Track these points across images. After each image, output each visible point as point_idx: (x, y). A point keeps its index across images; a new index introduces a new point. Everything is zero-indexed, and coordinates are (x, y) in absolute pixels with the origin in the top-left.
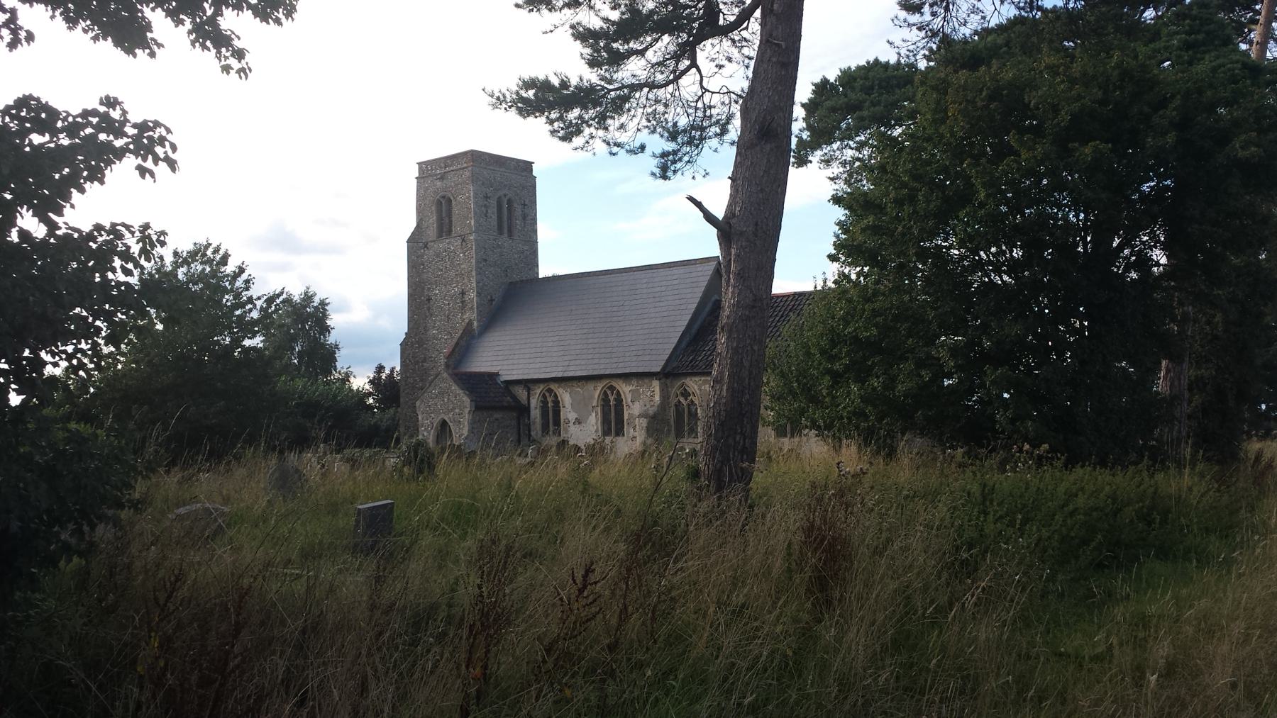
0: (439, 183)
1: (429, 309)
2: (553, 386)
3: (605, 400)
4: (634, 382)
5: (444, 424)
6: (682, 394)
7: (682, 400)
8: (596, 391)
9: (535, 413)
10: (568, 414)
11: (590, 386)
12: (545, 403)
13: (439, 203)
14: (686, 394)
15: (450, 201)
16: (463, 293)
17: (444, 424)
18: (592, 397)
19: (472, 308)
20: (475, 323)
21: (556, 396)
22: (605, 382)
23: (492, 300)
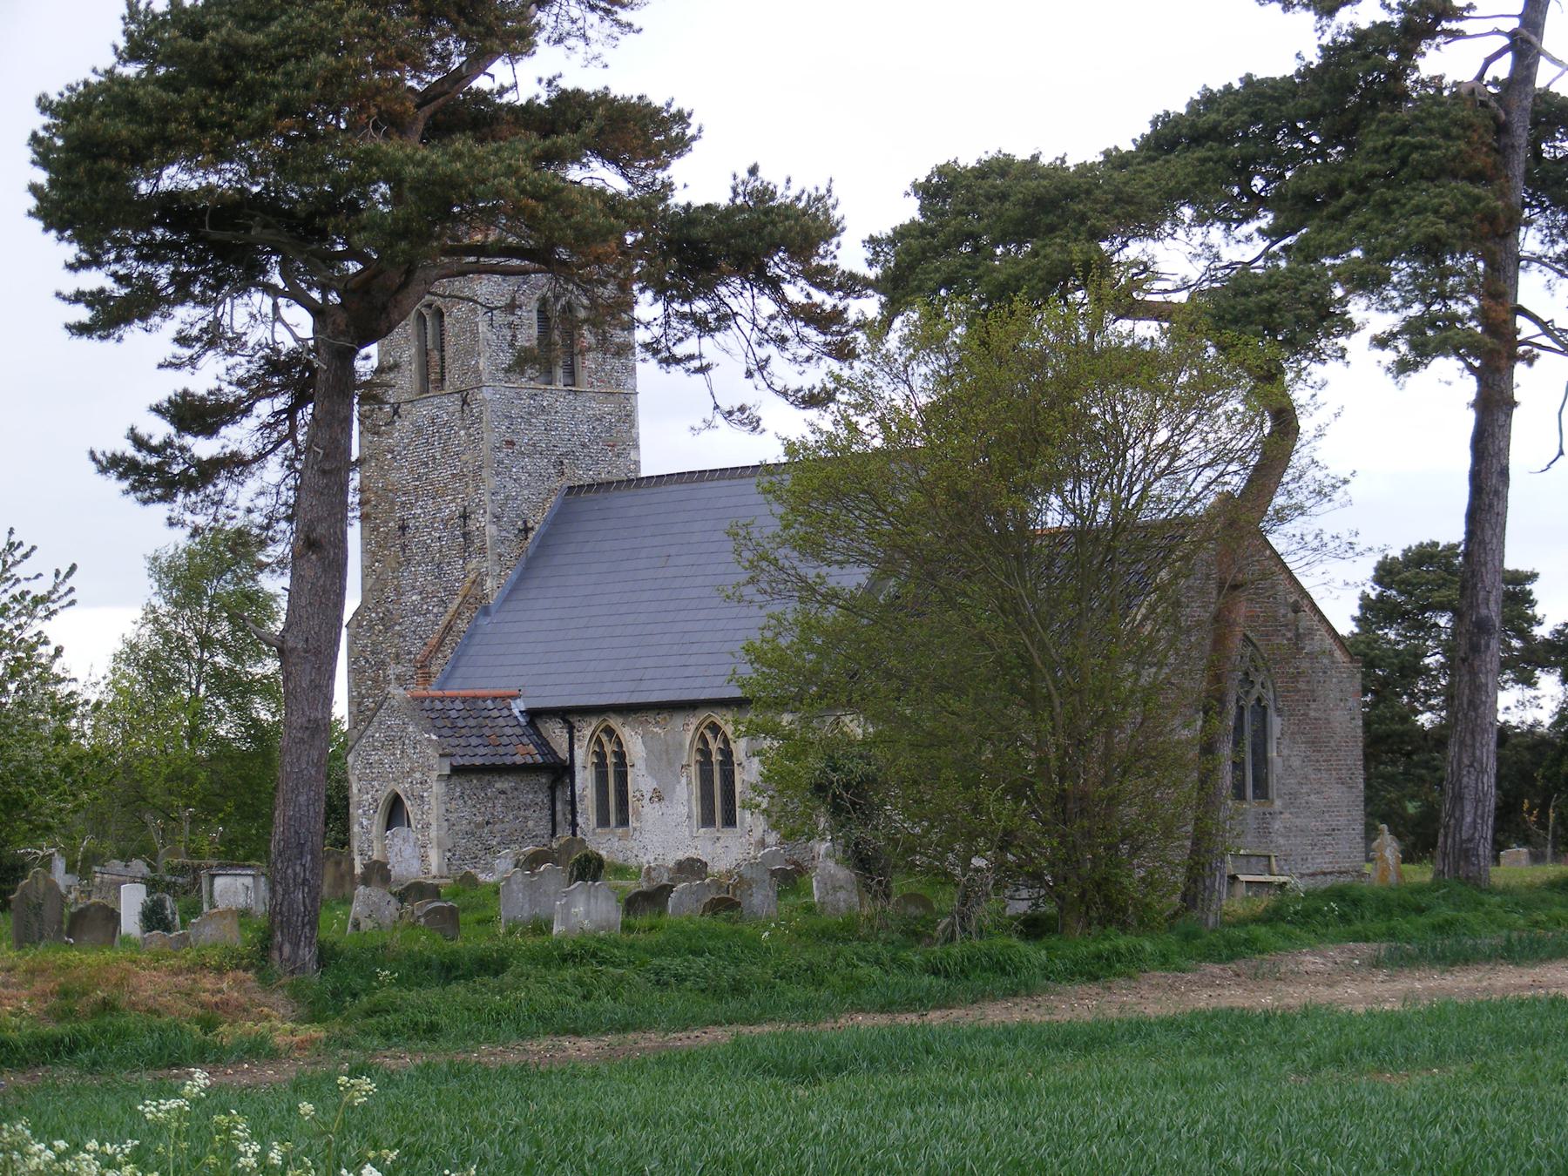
1: (404, 547)
2: (615, 722)
3: (705, 753)
8: (686, 730)
9: (584, 779)
10: (640, 780)
11: (678, 721)
12: (601, 755)
16: (465, 516)
18: (681, 745)
20: (489, 584)
21: (620, 744)
22: (703, 715)
23: (526, 530)
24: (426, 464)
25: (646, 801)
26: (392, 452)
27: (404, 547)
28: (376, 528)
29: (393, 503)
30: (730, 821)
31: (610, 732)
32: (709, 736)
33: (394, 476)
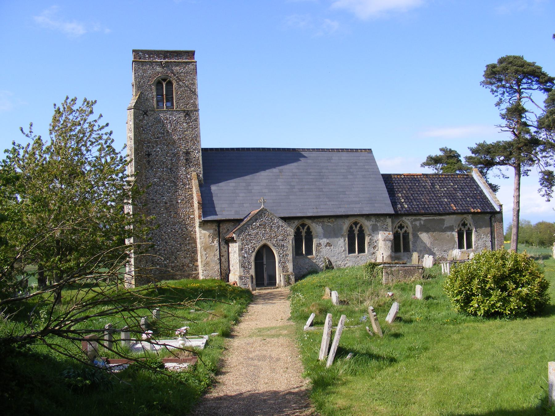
0: (159, 69)
1: (149, 162)
2: (308, 222)
4: (373, 219)
5: (265, 246)
6: (399, 227)
7: (399, 230)
11: (340, 221)
13: (159, 84)
14: (401, 227)
15: (170, 84)
17: (265, 247)
18: (341, 229)
19: (198, 164)
21: (309, 228)
22: (353, 220)
24: (163, 133)
25: (323, 246)
26: (142, 127)
27: (149, 162)
28: (138, 154)
29: (143, 146)
30: (362, 250)
31: (303, 225)
32: (354, 226)
33: (143, 136)
